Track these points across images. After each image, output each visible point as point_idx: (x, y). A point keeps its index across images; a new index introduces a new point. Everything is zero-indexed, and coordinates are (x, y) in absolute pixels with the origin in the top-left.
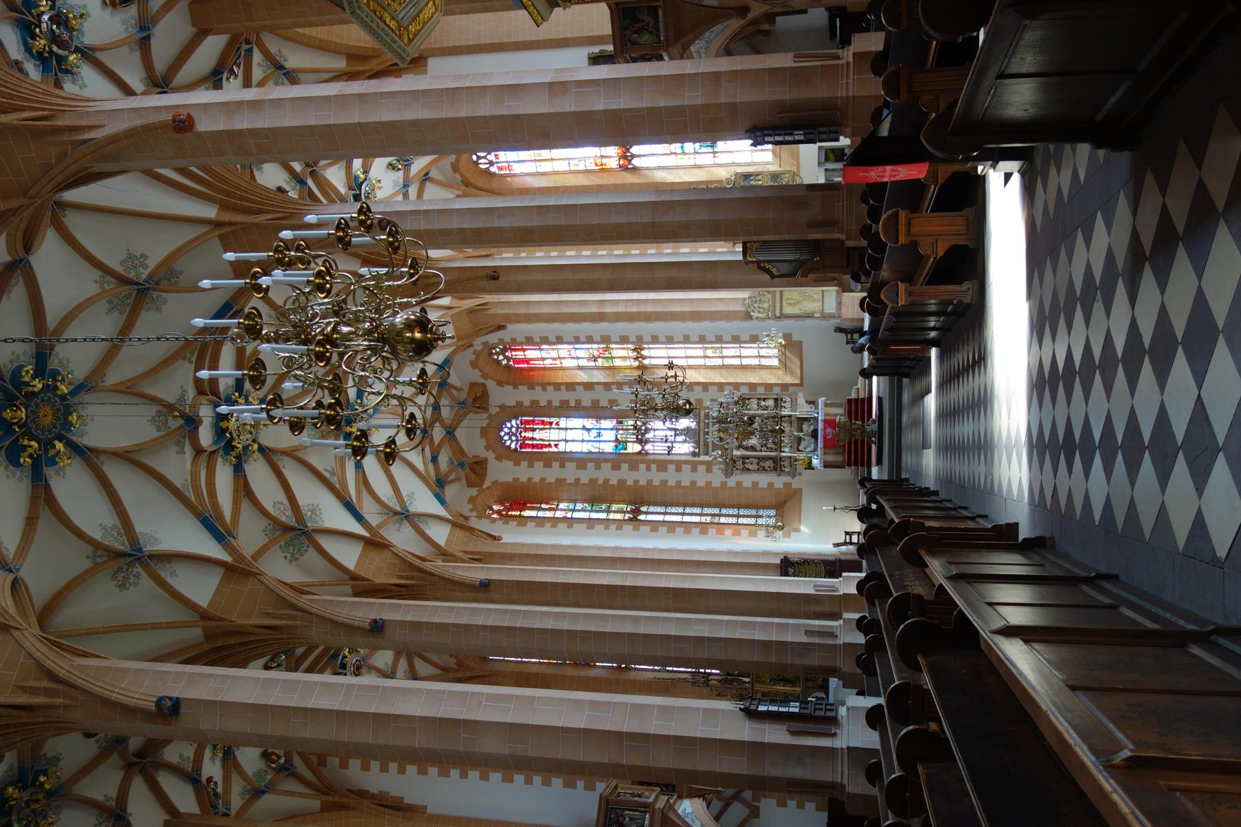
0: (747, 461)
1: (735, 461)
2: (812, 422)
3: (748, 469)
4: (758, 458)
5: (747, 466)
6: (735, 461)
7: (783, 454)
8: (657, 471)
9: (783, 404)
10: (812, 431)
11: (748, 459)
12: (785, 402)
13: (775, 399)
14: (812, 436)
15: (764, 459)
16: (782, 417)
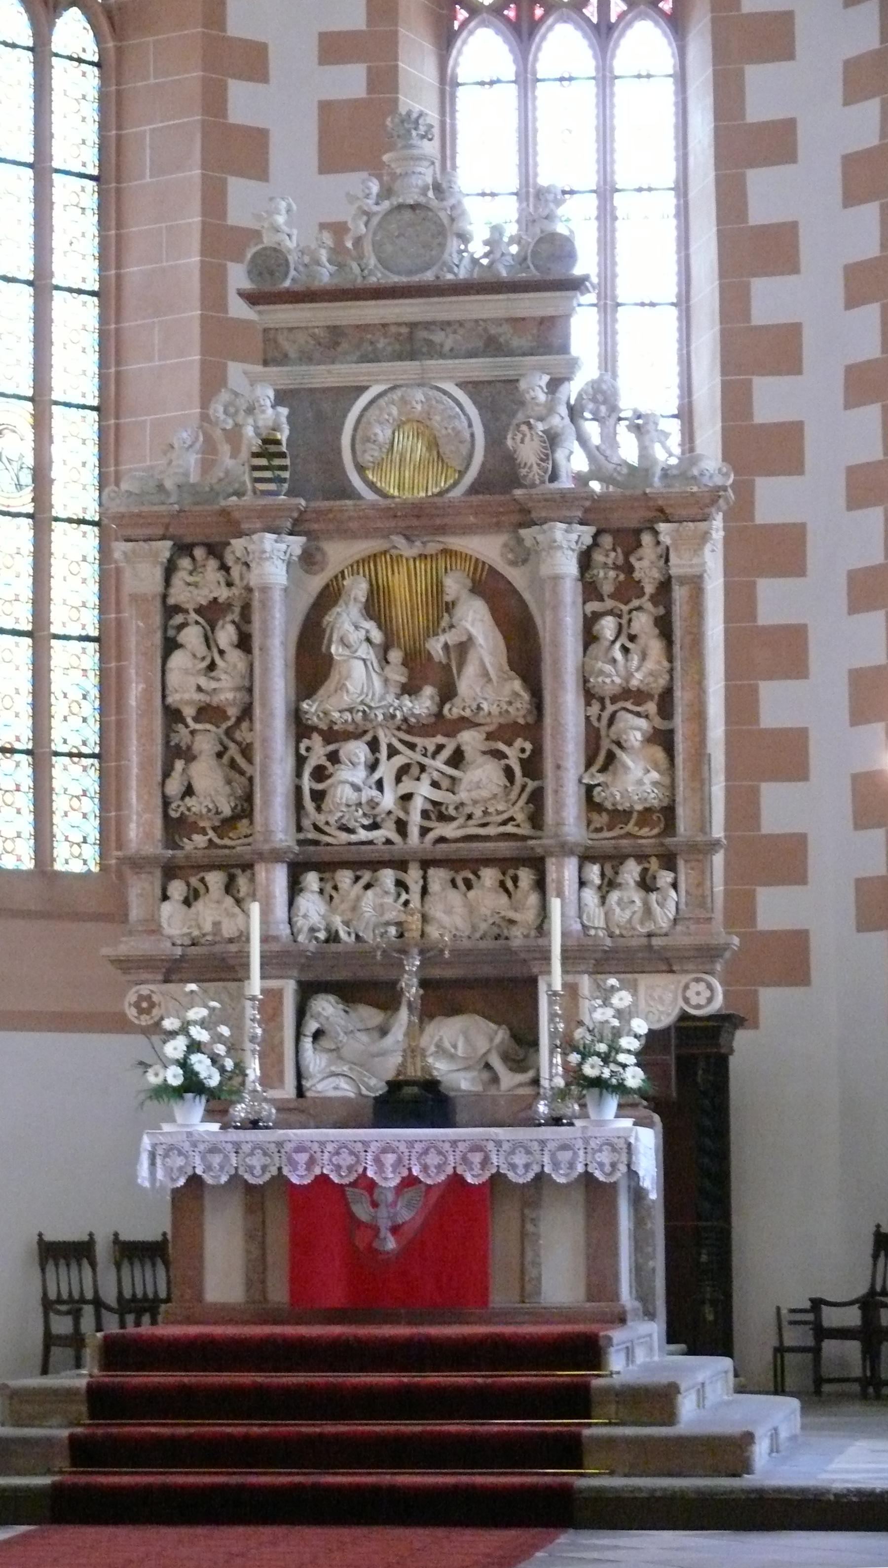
0: (226, 635)
1: (216, 550)
2: (509, 1080)
3: (170, 646)
4: (247, 712)
5: (192, 636)
6: (216, 550)
7: (280, 876)
8: (326, 108)
9: (631, 871)
10: (431, 1086)
11: (244, 643)
12: (646, 885)
13: (669, 812)
14: (394, 1086)
15: (247, 751)
16: (537, 864)
